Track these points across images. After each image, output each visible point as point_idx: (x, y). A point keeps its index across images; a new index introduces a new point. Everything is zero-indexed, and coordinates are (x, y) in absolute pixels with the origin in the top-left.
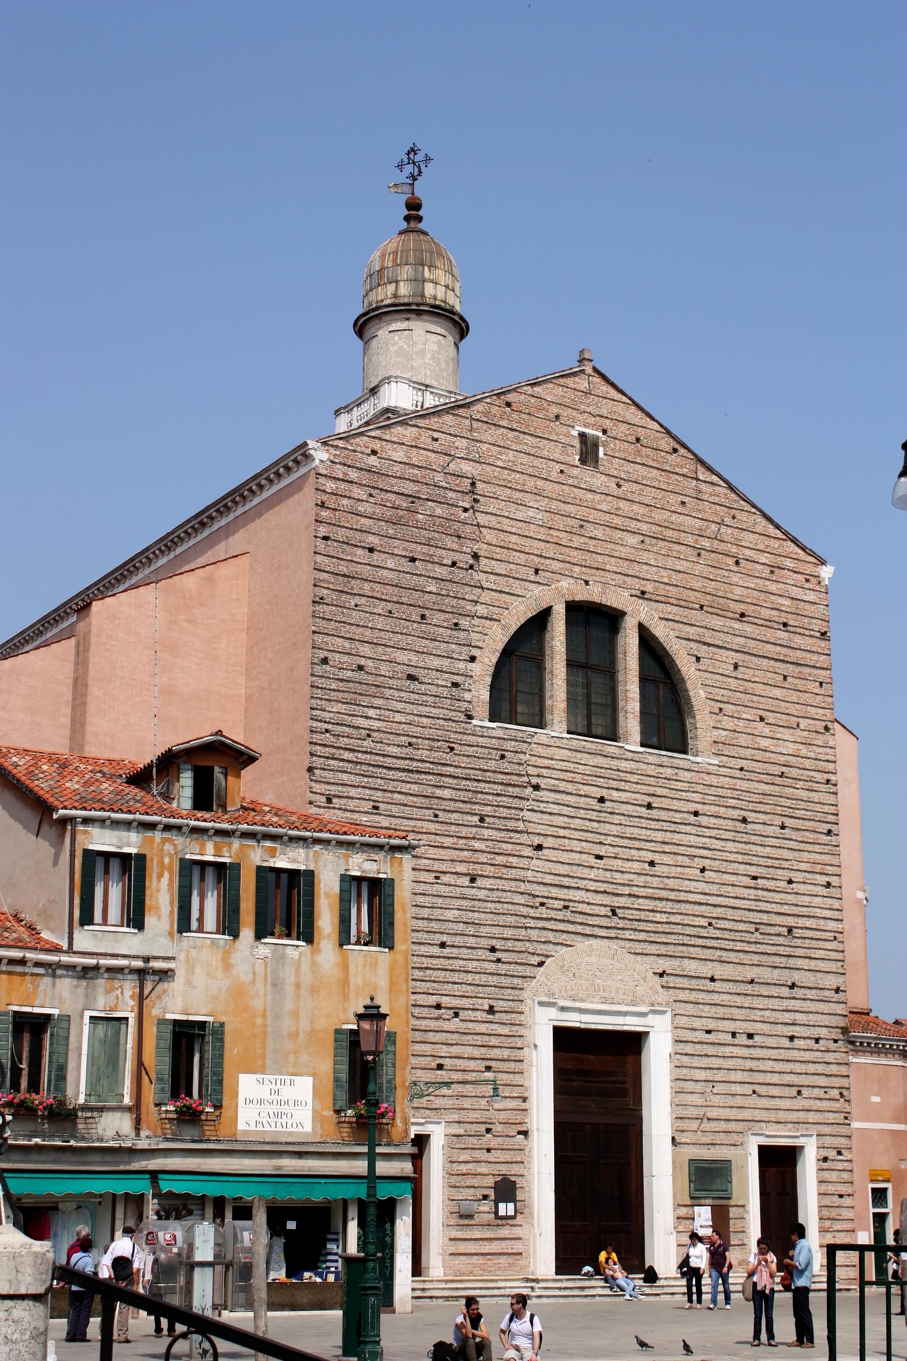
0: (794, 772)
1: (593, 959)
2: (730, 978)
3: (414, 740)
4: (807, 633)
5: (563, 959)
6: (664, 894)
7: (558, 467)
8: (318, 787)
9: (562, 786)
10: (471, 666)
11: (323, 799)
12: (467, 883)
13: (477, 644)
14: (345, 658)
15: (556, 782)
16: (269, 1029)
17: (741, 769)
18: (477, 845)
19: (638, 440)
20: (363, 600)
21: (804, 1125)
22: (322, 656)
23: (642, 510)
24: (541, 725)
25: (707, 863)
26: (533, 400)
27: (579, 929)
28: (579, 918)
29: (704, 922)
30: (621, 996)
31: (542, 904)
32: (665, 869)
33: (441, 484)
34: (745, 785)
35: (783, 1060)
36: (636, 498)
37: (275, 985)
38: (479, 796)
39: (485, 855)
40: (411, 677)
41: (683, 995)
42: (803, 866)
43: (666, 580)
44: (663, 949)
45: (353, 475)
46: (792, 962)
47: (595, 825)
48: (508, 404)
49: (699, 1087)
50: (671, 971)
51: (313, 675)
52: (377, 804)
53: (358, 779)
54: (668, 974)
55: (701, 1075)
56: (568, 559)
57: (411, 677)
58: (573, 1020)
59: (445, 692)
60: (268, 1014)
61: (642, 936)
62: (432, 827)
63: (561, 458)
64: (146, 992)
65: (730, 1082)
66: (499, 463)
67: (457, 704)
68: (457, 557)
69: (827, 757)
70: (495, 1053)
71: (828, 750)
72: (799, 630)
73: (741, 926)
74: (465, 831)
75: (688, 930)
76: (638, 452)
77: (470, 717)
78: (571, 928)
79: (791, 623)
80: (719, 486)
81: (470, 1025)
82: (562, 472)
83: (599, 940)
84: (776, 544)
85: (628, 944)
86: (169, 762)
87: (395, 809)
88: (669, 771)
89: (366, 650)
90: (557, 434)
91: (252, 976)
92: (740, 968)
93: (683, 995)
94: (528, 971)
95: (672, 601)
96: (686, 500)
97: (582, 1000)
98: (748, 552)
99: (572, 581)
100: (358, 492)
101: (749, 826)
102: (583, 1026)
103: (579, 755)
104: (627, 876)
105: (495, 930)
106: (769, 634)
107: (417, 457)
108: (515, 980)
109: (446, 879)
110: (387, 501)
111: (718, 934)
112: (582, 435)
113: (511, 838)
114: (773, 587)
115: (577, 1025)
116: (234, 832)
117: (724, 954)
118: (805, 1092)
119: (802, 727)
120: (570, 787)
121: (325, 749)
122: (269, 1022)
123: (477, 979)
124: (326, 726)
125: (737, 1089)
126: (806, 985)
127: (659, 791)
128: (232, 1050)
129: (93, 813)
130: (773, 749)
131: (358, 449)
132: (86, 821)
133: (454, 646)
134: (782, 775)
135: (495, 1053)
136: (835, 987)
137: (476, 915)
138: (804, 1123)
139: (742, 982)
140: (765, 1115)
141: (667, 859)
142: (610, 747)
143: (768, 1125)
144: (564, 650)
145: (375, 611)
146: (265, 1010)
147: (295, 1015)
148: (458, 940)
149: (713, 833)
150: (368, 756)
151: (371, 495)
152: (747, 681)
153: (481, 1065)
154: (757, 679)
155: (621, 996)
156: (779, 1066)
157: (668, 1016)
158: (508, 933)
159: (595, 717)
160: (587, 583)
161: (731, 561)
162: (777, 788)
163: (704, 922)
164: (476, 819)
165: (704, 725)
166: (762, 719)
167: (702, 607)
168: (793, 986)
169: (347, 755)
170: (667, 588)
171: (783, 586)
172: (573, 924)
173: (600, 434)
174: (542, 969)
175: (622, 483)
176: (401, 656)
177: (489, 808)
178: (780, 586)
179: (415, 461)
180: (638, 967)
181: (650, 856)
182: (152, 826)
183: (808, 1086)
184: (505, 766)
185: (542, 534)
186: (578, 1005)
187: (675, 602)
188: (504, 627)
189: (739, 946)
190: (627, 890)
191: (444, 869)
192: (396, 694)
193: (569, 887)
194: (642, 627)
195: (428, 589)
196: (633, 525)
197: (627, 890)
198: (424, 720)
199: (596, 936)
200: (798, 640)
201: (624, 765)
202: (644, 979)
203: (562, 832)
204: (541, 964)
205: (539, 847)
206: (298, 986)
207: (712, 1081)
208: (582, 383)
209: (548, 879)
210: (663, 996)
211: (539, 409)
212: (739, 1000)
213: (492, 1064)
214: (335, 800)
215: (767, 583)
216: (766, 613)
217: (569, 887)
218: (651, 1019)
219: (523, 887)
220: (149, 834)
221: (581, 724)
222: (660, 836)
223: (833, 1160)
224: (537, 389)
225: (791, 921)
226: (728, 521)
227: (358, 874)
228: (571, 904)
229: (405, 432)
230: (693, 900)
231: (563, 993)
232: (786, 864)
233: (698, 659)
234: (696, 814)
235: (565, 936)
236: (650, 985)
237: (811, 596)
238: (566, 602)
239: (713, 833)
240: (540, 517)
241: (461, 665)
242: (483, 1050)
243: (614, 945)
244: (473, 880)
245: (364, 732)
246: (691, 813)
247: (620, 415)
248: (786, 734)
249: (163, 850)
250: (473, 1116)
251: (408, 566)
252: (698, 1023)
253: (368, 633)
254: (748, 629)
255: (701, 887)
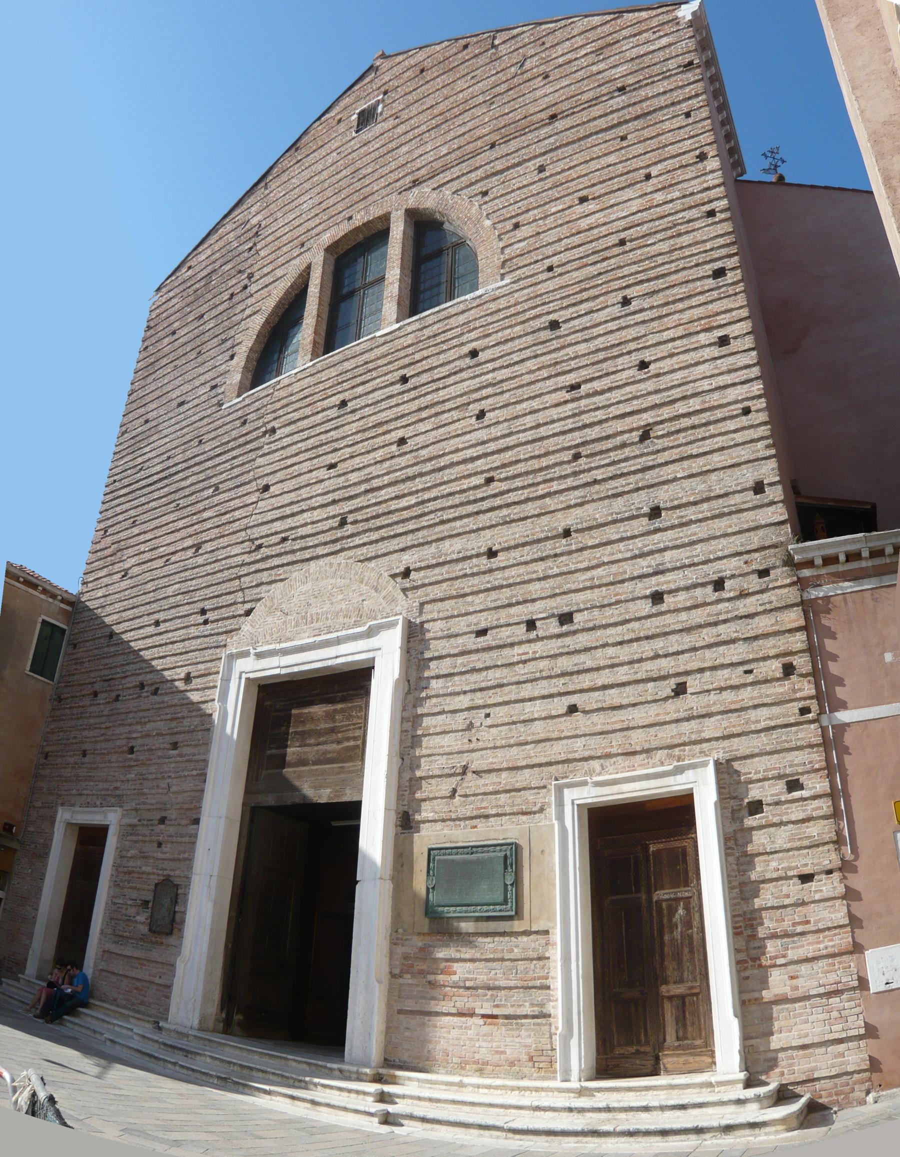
2: (523, 540)
21: (697, 748)
35: (638, 639)
44: (408, 540)
46: (650, 477)
49: (460, 720)
50: (418, 565)
54: (416, 570)
55: (464, 701)
65: (523, 701)
83: (321, 562)
97: (289, 639)
102: (284, 671)
111: (504, 486)
115: (276, 672)
118: (693, 683)
125: (537, 709)
126: (684, 501)
136: (750, 483)
138: (695, 742)
139: (547, 539)
140: (597, 745)
143: (607, 762)
152: (559, 173)
155: (341, 620)
156: (624, 652)
168: (655, 512)
172: (287, 551)
183: (701, 670)
193: (293, 515)
199: (317, 557)
204: (248, 613)
207: (484, 707)
212: (540, 568)
217: (293, 515)
223: (777, 803)
230: (460, 459)
231: (268, 637)
236: (384, 593)
243: (341, 558)
246: (466, 356)
252: (461, 625)
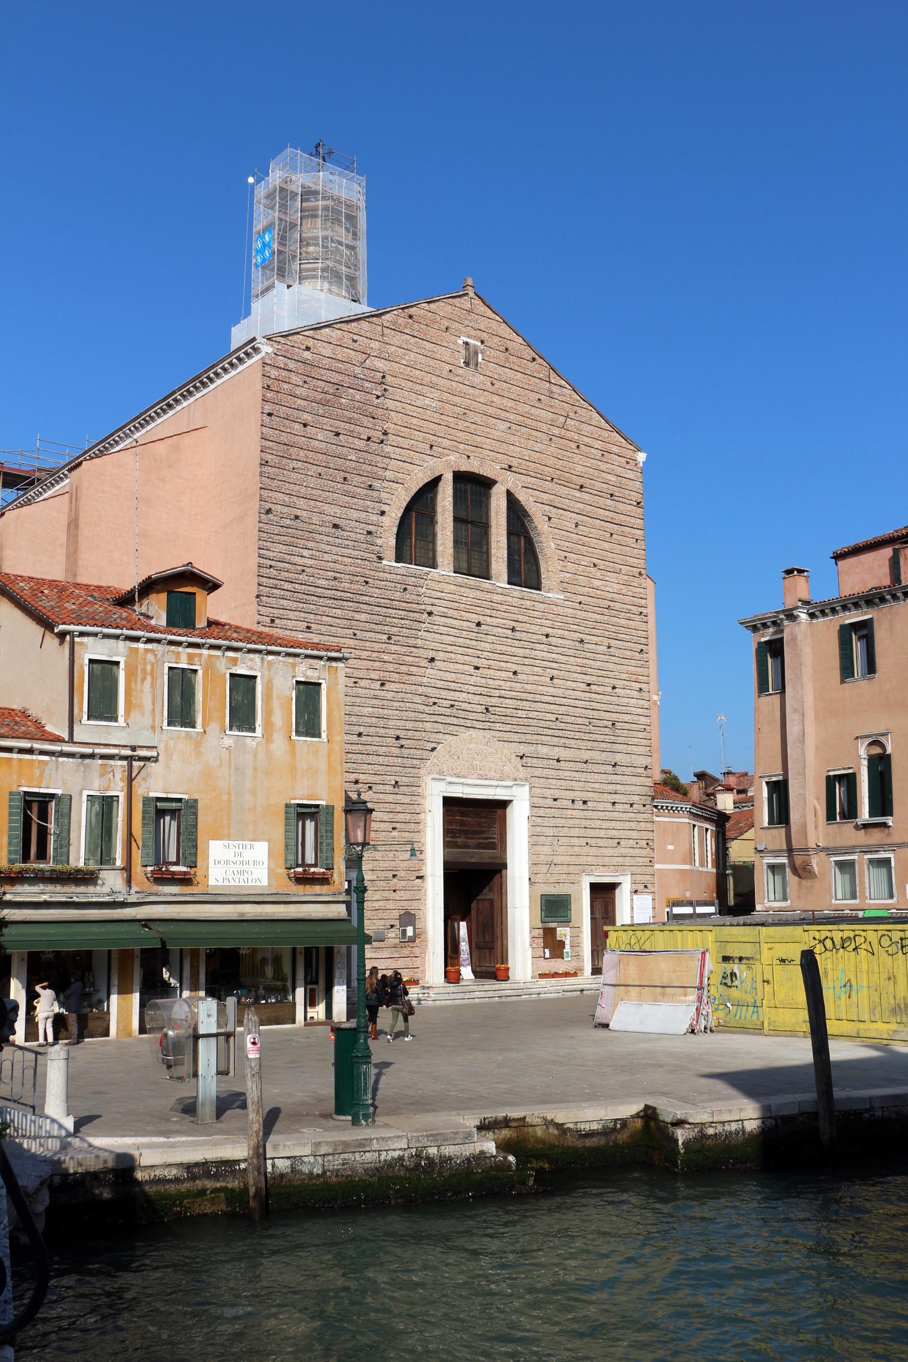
0: (617, 606)
1: (472, 746)
3: (338, 575)
4: (628, 502)
5: (450, 746)
6: (523, 696)
7: (448, 367)
8: (264, 610)
9: (450, 613)
10: (383, 518)
11: (268, 620)
12: (378, 687)
13: (387, 501)
14: (286, 510)
15: (446, 610)
16: (233, 804)
17: (580, 603)
18: (386, 657)
19: (507, 349)
20: (300, 464)
22: (267, 507)
23: (510, 404)
24: (434, 566)
25: (555, 673)
26: (429, 314)
27: (462, 722)
28: (462, 714)
29: (553, 717)
30: (493, 774)
31: (435, 704)
32: (524, 677)
33: (359, 376)
34: (582, 614)
36: (506, 394)
37: (237, 769)
38: (388, 619)
39: (392, 665)
40: (335, 526)
41: (538, 772)
42: (624, 676)
43: (527, 458)
44: (523, 738)
45: (292, 365)
47: (474, 643)
48: (411, 317)
51: (260, 522)
52: (310, 625)
53: (295, 605)
56: (455, 438)
57: (335, 526)
58: (458, 792)
59: (362, 537)
60: (232, 792)
61: (508, 728)
62: (352, 643)
63: (451, 361)
64: (133, 776)
66: (404, 362)
67: (372, 547)
68: (371, 433)
69: (641, 596)
70: (400, 817)
71: (641, 590)
72: (621, 499)
73: (580, 721)
74: (377, 646)
75: (542, 724)
76: (507, 359)
77: (380, 558)
78: (455, 721)
79: (617, 494)
81: (381, 796)
82: (450, 371)
84: (606, 434)
85: (498, 734)
86: (148, 587)
87: (324, 629)
88: (528, 603)
89: (301, 503)
90: (448, 342)
91: (219, 761)
92: (579, 752)
93: (538, 772)
94: (425, 754)
95: (531, 473)
96: (542, 397)
97: (465, 777)
98: (585, 439)
99: (458, 455)
100: (295, 379)
101: (586, 646)
103: (463, 590)
104: (497, 683)
105: (400, 723)
106: (601, 501)
107: (341, 353)
108: (415, 762)
109: (362, 683)
110: (318, 387)
111: (563, 726)
112: (467, 344)
113: (411, 652)
114: (604, 467)
115: (460, 795)
116: (203, 645)
117: (567, 741)
119: (623, 572)
120: (455, 614)
121: (271, 578)
122: (233, 798)
123: (385, 760)
124: (270, 562)
127: (521, 618)
128: (204, 820)
129: (88, 629)
130: (602, 588)
131: (296, 345)
132: (82, 634)
133: (369, 503)
134: (609, 608)
135: (400, 817)
137: (385, 711)
142: (485, 584)
144: (451, 508)
145: (309, 473)
146: (229, 789)
147: (254, 793)
148: (372, 730)
149: (560, 650)
150: (303, 587)
151: (305, 382)
153: (389, 826)
154: (591, 535)
155: (493, 774)
157: (527, 788)
158: (409, 725)
159: (473, 561)
160: (468, 457)
161: (574, 445)
162: (606, 618)
163: (553, 717)
164: (385, 637)
166: (595, 566)
167: (552, 479)
169: (287, 586)
170: (528, 463)
171: (611, 466)
172: (456, 717)
173: (479, 344)
174: (435, 753)
175: (495, 381)
176: (327, 508)
177: (395, 629)
178: (609, 466)
179: (339, 357)
180: (505, 751)
181: (514, 667)
182: (136, 639)
184: (407, 596)
185: (436, 418)
186: (461, 780)
187: (533, 474)
188: (406, 490)
189: (578, 735)
190: (497, 693)
191: (361, 676)
192: (325, 538)
194: (509, 494)
195: (349, 458)
196: (504, 414)
197: (497, 693)
198: (346, 559)
200: (621, 506)
201: (496, 598)
202: (510, 760)
203: (449, 648)
204: (433, 749)
205: (432, 660)
206: (255, 769)
208: (465, 303)
209: (440, 684)
210: (522, 773)
211: (434, 322)
213: (398, 825)
214: (277, 621)
215: (600, 463)
216: (599, 486)
219: (421, 690)
220: (134, 645)
221: (464, 565)
222: (521, 652)
224: (432, 305)
225: (614, 717)
226: (572, 415)
227: (303, 680)
228: (456, 703)
229: (332, 334)
232: (611, 674)
233: (550, 519)
234: (547, 636)
235: (452, 728)
237: (631, 475)
238: (454, 472)
239: (560, 650)
240: (434, 405)
241: (375, 518)
242: (391, 815)
245: (300, 568)
247: (494, 330)
248: (612, 577)
249: (145, 659)
250: (383, 865)
251: (335, 440)
252: (548, 793)
253: (303, 490)
254: (586, 497)
255: (551, 690)
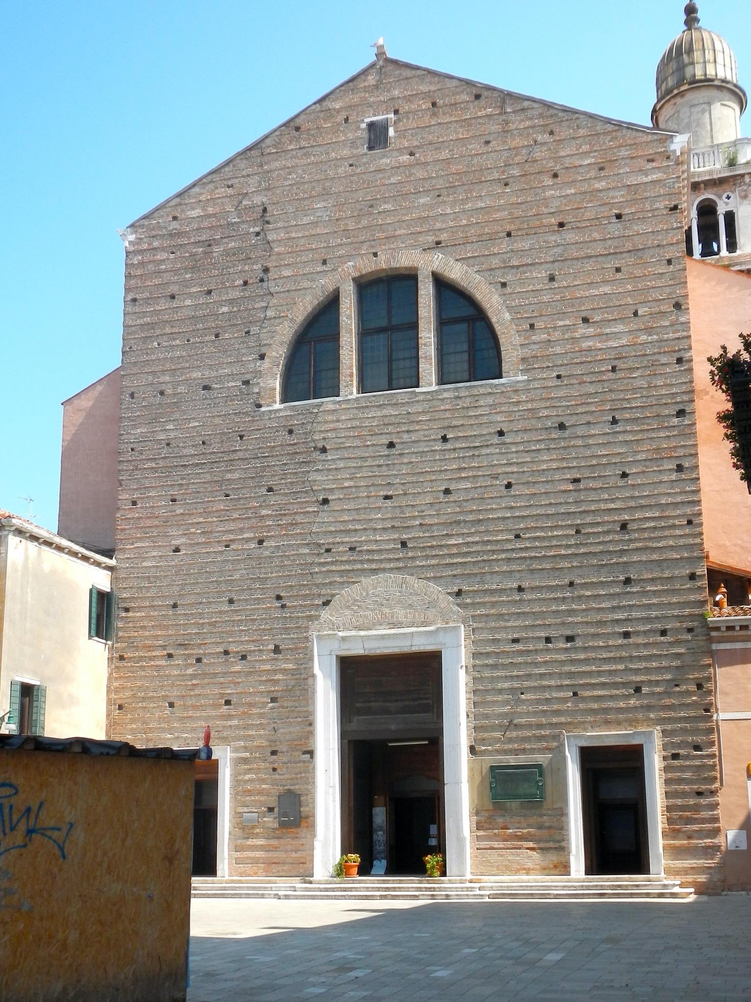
80: (533, 108)
141: (463, 485)
165: (511, 345)
172: (359, 562)
176: (197, 374)
199: (384, 570)
204: (326, 603)
218: (441, 638)
238: (354, 279)
244: (261, 542)
